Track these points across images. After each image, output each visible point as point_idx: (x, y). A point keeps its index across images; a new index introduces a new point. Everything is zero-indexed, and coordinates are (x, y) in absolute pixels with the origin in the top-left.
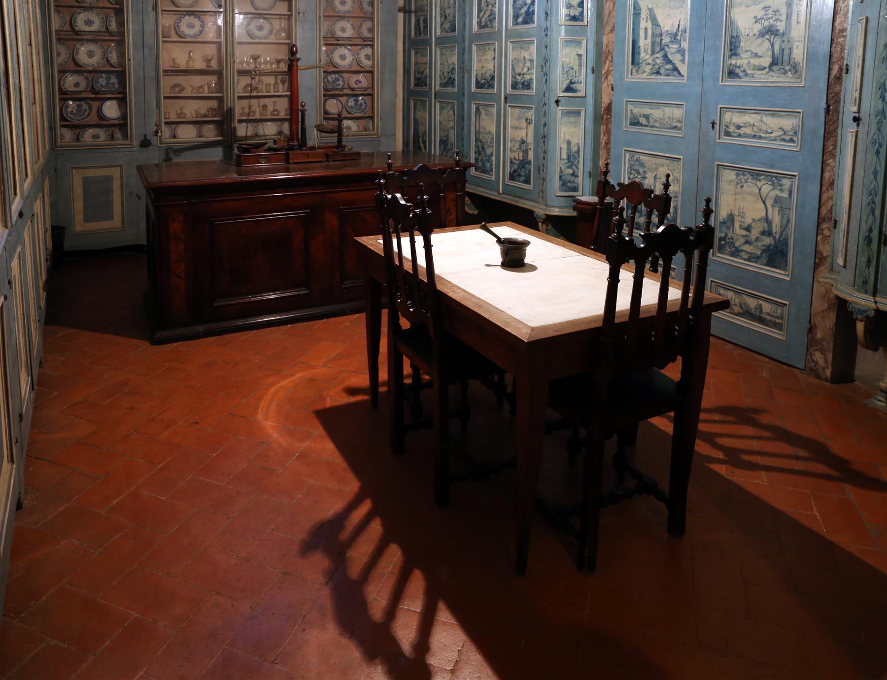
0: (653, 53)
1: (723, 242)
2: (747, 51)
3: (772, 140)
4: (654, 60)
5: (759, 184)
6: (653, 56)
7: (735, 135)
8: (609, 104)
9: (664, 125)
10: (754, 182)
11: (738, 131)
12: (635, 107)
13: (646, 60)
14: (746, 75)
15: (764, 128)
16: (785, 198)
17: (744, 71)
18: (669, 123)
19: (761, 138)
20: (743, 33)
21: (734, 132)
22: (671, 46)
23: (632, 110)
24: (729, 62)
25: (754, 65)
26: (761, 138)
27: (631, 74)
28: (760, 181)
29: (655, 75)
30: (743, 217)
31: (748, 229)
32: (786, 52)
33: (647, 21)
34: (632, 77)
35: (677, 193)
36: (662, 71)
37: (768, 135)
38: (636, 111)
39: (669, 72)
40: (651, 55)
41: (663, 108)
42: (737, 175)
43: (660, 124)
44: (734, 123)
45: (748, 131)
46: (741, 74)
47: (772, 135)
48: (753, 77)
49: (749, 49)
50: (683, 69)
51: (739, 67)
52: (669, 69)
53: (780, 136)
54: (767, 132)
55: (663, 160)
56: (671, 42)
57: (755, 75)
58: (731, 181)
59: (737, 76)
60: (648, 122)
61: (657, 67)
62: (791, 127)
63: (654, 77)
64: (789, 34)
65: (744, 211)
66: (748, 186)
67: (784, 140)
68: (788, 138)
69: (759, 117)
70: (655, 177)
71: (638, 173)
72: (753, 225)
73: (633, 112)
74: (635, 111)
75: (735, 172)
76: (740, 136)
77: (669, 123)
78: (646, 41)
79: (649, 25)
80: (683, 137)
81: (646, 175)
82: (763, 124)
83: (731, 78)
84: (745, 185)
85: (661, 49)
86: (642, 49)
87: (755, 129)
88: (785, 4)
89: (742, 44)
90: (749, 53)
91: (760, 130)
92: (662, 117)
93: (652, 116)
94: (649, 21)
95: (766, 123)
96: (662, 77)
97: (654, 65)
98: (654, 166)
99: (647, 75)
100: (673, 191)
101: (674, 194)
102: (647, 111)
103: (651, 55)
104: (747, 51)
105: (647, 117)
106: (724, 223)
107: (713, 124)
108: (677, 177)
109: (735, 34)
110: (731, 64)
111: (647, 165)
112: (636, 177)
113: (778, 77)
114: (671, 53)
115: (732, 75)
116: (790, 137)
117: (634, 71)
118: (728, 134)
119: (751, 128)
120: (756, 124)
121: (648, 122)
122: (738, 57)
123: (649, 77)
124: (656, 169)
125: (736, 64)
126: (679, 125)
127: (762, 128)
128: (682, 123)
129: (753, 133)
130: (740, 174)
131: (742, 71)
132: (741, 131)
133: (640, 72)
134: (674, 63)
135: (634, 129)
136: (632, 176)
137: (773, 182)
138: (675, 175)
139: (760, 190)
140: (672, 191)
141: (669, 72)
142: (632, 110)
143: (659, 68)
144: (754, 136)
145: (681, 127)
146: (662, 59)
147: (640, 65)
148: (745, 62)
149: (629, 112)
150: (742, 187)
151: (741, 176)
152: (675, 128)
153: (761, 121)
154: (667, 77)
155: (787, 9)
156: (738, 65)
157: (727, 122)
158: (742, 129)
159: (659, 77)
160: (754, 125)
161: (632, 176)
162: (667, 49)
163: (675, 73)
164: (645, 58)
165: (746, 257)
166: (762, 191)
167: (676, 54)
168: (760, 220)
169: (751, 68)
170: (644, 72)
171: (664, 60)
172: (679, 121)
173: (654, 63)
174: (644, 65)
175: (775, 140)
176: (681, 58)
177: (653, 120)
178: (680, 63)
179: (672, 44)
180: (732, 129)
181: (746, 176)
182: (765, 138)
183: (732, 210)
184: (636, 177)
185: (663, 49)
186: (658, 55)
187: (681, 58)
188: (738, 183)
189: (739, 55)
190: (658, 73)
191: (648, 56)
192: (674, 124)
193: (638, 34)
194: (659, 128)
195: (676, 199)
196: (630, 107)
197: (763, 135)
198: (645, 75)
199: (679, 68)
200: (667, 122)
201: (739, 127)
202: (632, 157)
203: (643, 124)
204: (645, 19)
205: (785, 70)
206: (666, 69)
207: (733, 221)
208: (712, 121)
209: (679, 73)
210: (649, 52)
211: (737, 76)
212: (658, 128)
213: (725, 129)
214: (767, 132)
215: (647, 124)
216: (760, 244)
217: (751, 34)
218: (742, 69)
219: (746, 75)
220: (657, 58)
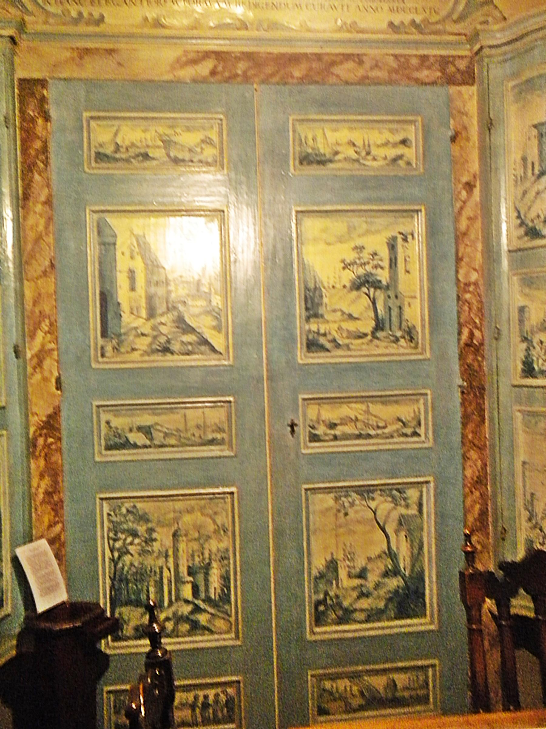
0: (151, 314)
1: (322, 608)
2: (334, 311)
3: (387, 438)
4: (154, 328)
5: (373, 505)
6: (152, 321)
7: (327, 438)
8: (49, 416)
9: (189, 439)
10: (364, 502)
11: (332, 432)
12: (115, 416)
13: (136, 328)
14: (338, 346)
15: (373, 421)
16: (414, 516)
17: (334, 341)
18: (197, 435)
19: (369, 436)
20: (326, 285)
21: (326, 434)
22: (190, 302)
23: (108, 423)
24: (307, 327)
25: (348, 331)
26: (369, 436)
27: (103, 355)
28: (373, 499)
29: (160, 354)
30: (352, 560)
31: (362, 575)
32: (395, 313)
33: (132, 258)
34: (105, 359)
35: (227, 550)
36: (176, 346)
37: (379, 432)
38: (118, 422)
39: (190, 348)
40: (148, 319)
41: (183, 411)
42: (337, 499)
43: (179, 440)
44: (323, 421)
45: (349, 429)
46: (328, 345)
47: (386, 431)
48: (349, 349)
49: (338, 307)
50: (218, 341)
51: (325, 335)
52: (190, 343)
53: (397, 430)
54: (378, 427)
55: (188, 502)
56: (194, 297)
57: (351, 347)
58: (328, 510)
59: (322, 348)
60: (151, 439)
61: (163, 339)
62: (412, 415)
63: (158, 357)
64: (396, 287)
65: (353, 550)
66: (356, 512)
67: (406, 435)
68: (409, 431)
69: (364, 407)
70: (175, 535)
71: (135, 534)
72: (369, 567)
73: (112, 425)
74: (116, 422)
75: (332, 495)
76: (335, 438)
77: (197, 435)
78: (132, 294)
79: (138, 265)
80: (236, 456)
81: (154, 535)
82: (370, 417)
83: (311, 355)
84: (351, 512)
85: (168, 309)
86: (125, 307)
87: (359, 425)
88: (386, 245)
89: (325, 300)
90: (339, 314)
91: (367, 425)
92: (181, 427)
93: (159, 427)
94: (139, 258)
95: (374, 413)
96: (176, 357)
97: (155, 337)
98: (172, 515)
99: (142, 355)
100: (218, 550)
101: (219, 555)
102: (146, 420)
103: (148, 319)
104: (334, 311)
105: (146, 431)
106: (322, 576)
107: (292, 426)
108: (223, 525)
109: (311, 285)
110: (310, 331)
111: (155, 517)
112: (131, 543)
113: (386, 347)
114: (193, 316)
115: (313, 348)
116: (412, 430)
117: (109, 348)
118: (314, 438)
119: (353, 424)
120: (360, 417)
121: (151, 439)
122: (320, 320)
123: (146, 358)
124: (176, 520)
125: (318, 330)
126: (219, 436)
127: (371, 422)
128: (224, 431)
129: (357, 432)
130: (340, 496)
131: (329, 341)
132: (338, 431)
133: (122, 350)
134: (199, 333)
135: (118, 455)
136: (118, 545)
137: (393, 497)
138: (219, 522)
139: (375, 513)
140: (214, 549)
141: (190, 348)
142: (108, 423)
143: (168, 341)
144: (359, 436)
145: (223, 439)
146: (174, 325)
147: (123, 337)
148: (336, 326)
149: (103, 425)
150: (346, 514)
151: (343, 499)
152: (212, 442)
153: (368, 412)
154: (187, 357)
155: (390, 254)
156: (322, 331)
157: (312, 420)
158: (339, 427)
159: (169, 357)
160: (357, 419)
161: (118, 545)
162: (181, 308)
163: (203, 348)
164: (135, 325)
165: (361, 616)
166: (379, 513)
167: (203, 317)
168: (380, 556)
169: (344, 335)
170: (133, 350)
171: (178, 327)
172: (220, 430)
173: (155, 333)
174: (131, 338)
175: (392, 437)
176: (214, 323)
177: (162, 435)
178: (213, 332)
179: (193, 300)
180: (321, 430)
181: (350, 496)
182: (377, 436)
183: (332, 554)
184: (131, 543)
185: (175, 308)
186: (163, 320)
187: (214, 323)
188: (339, 511)
189: (322, 316)
190: (166, 350)
191: (141, 321)
192: (210, 436)
193: (113, 281)
194: (177, 446)
195: (226, 562)
196: (104, 417)
197: (372, 432)
198: (136, 356)
199: (209, 340)
200: (194, 435)
201: (333, 426)
202: (115, 510)
203: (139, 444)
204: (128, 254)
205: (396, 337)
206: (183, 342)
207: (336, 570)
208: (290, 423)
209: (213, 350)
210: (144, 313)
211: (322, 348)
212: (173, 446)
213: (310, 432)
214: (378, 427)
215: (148, 442)
216: (382, 592)
217: (338, 286)
218: (330, 337)
219: (338, 346)
220: (162, 324)
